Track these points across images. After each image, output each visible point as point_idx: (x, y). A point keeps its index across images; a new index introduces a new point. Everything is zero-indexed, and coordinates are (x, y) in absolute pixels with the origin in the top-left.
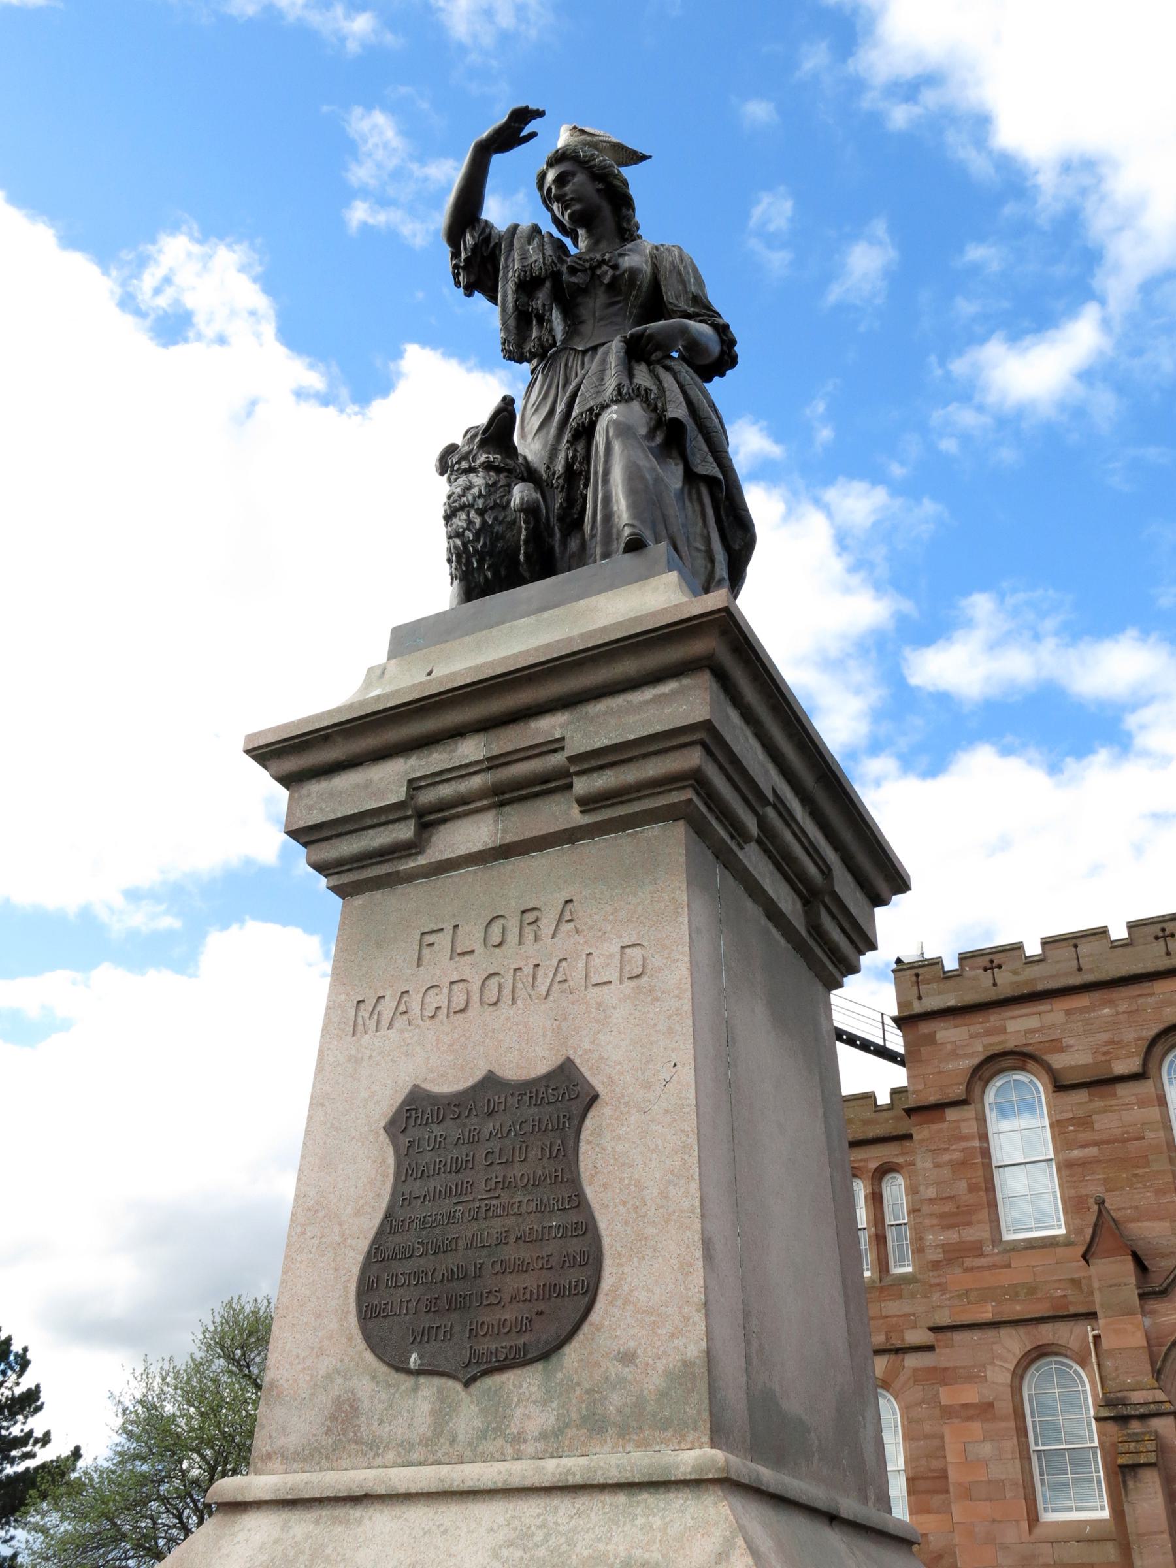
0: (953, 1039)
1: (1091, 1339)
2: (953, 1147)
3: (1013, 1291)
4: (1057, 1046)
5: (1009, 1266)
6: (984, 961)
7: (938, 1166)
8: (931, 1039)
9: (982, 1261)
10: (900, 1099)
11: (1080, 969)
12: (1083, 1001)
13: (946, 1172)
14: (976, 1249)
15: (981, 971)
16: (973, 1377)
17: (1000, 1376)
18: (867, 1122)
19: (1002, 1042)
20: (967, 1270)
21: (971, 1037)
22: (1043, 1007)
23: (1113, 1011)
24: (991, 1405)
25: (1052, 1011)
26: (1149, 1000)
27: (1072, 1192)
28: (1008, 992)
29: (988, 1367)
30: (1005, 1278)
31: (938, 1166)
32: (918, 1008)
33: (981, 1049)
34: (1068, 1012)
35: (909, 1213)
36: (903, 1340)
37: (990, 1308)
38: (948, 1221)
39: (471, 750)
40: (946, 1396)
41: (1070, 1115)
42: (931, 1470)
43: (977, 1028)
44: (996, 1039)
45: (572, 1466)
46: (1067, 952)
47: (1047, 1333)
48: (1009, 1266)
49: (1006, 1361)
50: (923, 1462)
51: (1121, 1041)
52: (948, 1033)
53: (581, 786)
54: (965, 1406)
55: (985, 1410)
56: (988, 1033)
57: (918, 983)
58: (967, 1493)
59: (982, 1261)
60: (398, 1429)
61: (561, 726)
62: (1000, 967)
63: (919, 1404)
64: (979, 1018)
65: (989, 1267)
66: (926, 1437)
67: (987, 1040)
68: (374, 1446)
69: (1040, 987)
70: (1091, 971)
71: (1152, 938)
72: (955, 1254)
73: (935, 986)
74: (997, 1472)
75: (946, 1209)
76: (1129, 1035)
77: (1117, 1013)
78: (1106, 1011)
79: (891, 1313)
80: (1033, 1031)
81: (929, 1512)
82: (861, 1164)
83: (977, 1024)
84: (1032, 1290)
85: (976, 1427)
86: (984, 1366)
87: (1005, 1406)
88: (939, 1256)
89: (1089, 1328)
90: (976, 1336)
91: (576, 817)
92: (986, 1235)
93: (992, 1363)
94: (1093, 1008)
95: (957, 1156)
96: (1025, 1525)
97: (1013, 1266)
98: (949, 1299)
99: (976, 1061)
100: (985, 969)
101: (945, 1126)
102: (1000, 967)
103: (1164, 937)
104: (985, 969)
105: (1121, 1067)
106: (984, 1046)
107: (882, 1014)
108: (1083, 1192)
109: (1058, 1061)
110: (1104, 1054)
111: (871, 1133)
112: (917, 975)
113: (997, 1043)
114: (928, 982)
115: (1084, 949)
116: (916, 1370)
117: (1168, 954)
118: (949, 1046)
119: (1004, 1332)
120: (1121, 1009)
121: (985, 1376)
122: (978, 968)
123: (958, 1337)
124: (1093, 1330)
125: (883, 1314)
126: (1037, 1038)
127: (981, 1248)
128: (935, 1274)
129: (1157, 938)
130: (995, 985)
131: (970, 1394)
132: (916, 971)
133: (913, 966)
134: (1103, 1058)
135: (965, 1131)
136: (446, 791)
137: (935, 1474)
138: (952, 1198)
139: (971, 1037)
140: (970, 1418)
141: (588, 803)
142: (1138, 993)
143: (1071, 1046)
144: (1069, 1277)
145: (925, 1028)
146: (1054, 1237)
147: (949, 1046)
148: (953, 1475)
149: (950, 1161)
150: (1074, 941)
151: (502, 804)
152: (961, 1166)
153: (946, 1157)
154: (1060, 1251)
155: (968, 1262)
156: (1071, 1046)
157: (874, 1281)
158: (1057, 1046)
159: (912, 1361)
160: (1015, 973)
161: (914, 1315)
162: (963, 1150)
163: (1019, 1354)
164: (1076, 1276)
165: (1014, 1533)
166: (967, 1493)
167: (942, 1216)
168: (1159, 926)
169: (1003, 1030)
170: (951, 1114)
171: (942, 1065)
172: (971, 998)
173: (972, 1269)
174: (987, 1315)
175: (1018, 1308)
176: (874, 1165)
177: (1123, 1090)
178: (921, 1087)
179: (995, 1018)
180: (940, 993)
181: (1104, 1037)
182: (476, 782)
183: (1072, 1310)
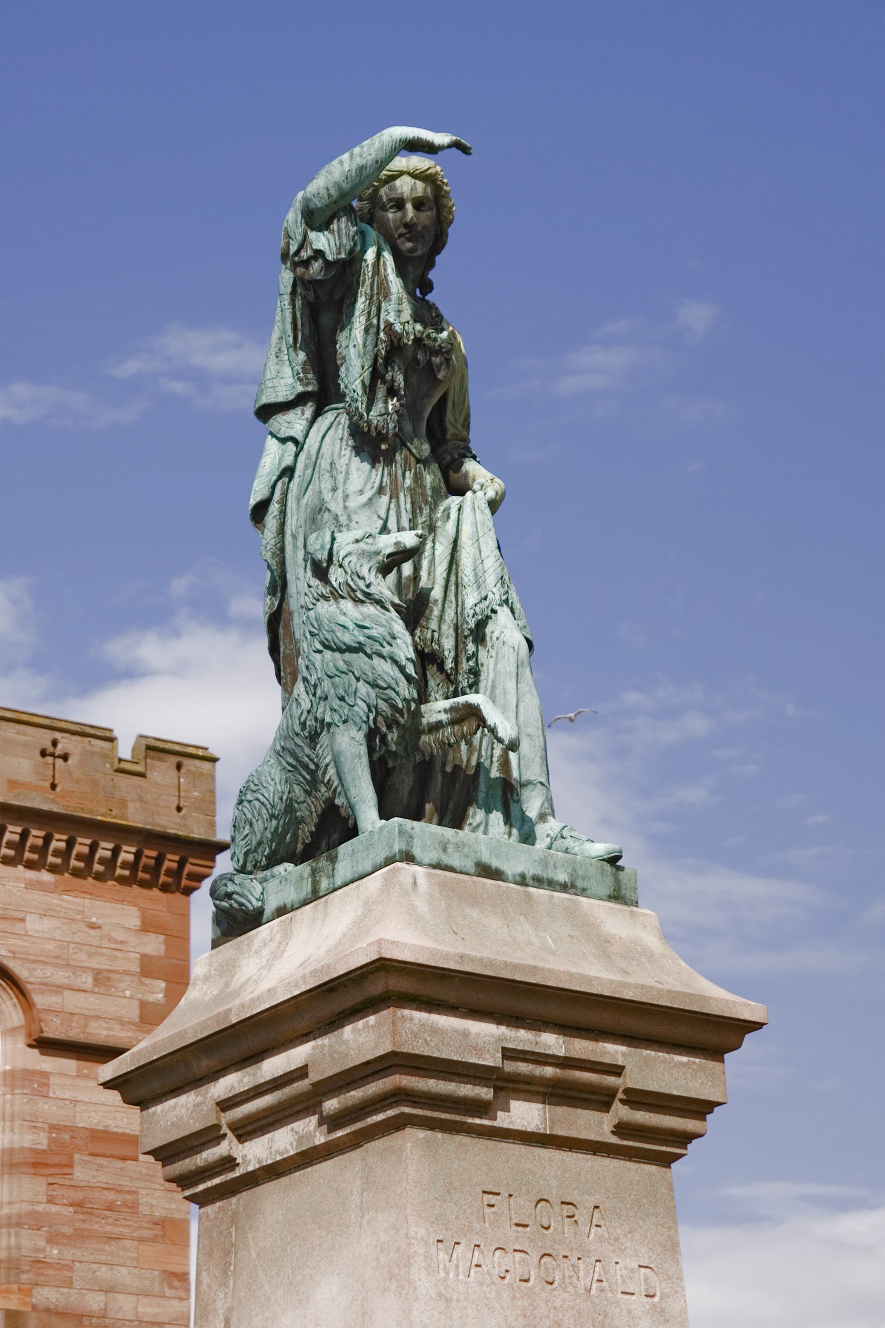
61: (624, 1055)
141: (622, 1129)
151: (551, 1095)
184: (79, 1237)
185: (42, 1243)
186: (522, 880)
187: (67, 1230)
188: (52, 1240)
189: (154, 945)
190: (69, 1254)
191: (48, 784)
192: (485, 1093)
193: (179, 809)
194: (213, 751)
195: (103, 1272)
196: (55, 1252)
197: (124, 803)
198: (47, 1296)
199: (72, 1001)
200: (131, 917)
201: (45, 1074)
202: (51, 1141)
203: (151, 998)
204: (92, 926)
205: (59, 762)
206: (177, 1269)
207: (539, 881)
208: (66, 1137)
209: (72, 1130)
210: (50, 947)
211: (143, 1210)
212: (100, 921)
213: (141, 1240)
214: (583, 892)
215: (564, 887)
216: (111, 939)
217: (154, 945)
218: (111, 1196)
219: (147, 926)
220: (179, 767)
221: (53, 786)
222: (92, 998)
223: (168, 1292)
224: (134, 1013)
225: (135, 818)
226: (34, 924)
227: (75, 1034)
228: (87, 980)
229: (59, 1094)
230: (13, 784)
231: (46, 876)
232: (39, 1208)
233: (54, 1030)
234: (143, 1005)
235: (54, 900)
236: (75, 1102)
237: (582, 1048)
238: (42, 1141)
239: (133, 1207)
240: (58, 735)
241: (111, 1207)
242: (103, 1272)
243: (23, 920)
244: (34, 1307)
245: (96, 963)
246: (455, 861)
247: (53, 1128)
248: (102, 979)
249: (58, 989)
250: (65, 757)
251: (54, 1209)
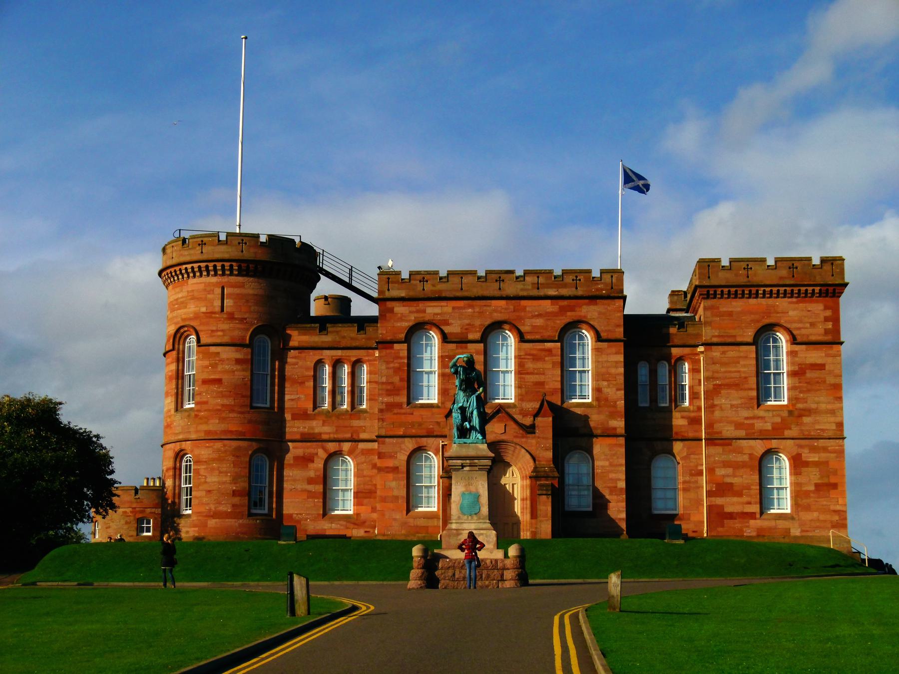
0: (402, 312)
1: (441, 446)
2: (395, 361)
3: (412, 425)
4: (447, 323)
5: (412, 414)
6: (419, 277)
7: (388, 368)
8: (391, 310)
9: (403, 411)
10: (369, 330)
11: (462, 289)
12: (461, 303)
13: (391, 371)
14: (399, 405)
15: (418, 282)
16: (392, 456)
17: (403, 457)
18: (352, 339)
19: (422, 317)
20: (395, 414)
21: (411, 312)
22: (443, 303)
23: (473, 311)
24: (397, 468)
25: (447, 306)
26: (488, 308)
27: (443, 386)
28: (430, 295)
29: (398, 454)
30: (410, 419)
31: (388, 368)
32: (388, 295)
33: (413, 318)
34: (454, 308)
35: (367, 382)
36: (359, 437)
37: (402, 430)
38: (389, 393)
39: (468, 461)
40: (379, 463)
41: (447, 354)
42: (365, 489)
43: (413, 309)
44: (421, 315)
45: (477, 522)
46: (456, 280)
47: (424, 441)
48: (412, 414)
49: (405, 451)
50: (362, 486)
51: (473, 325)
52: (400, 309)
53: (478, 467)
54: (387, 468)
55: (395, 469)
56: (418, 312)
57: (389, 282)
58: (384, 500)
59: (403, 411)
60: (464, 518)
62: (427, 281)
63: (363, 463)
64: (415, 303)
65: (404, 414)
66: (364, 476)
67: (416, 315)
68: (462, 519)
69: (443, 295)
70: (467, 291)
71: (495, 281)
72: (390, 407)
73: (396, 285)
74: (396, 493)
75: (389, 387)
76: (478, 322)
77: (474, 312)
78: (470, 310)
79: (355, 425)
80: (437, 314)
81: (362, 505)
82: (347, 358)
83: (414, 306)
84: (420, 424)
85: (391, 476)
86: (397, 453)
87: (403, 468)
88: (384, 407)
89: (441, 441)
90: (395, 440)
91: (477, 470)
92: (405, 400)
93: (400, 452)
94: (464, 308)
95: (397, 365)
96: (405, 512)
97: (414, 414)
98: (386, 425)
99: (411, 324)
100: (420, 281)
101: (393, 351)
102: (427, 281)
103: (500, 281)
104: (420, 281)
105: (471, 337)
106: (415, 317)
107: (352, 267)
108: (447, 387)
109: (447, 329)
110: (466, 329)
111: (354, 344)
112: (389, 278)
113: (421, 317)
114: (393, 282)
115: (464, 280)
116: (363, 450)
117: (500, 289)
118: (399, 315)
119: (406, 440)
120: (477, 310)
121: (396, 457)
122: (417, 280)
123: (387, 440)
124: (442, 442)
125: (351, 425)
126: (439, 317)
127: (402, 405)
128: (381, 414)
129: (497, 281)
130: (424, 289)
131: (391, 463)
132: (388, 276)
133: (387, 273)
134: (465, 331)
135: (401, 355)
136: (465, 464)
137: (367, 491)
138: (392, 383)
139: (411, 312)
140: (388, 472)
141: (479, 469)
142: (484, 304)
143: (453, 324)
144: (436, 420)
145: (389, 304)
146: (432, 404)
147: (399, 315)
148: (379, 493)
149: (393, 367)
150: (461, 275)
152: (397, 370)
153: (392, 365)
154: (434, 410)
155: (396, 411)
156: (453, 324)
157: (348, 411)
158: (447, 323)
159: (361, 446)
160: (434, 285)
161: (365, 427)
162: (399, 363)
163: (411, 449)
164: (439, 421)
165: (400, 515)
166: (384, 500)
167: (387, 390)
168: (499, 275)
169: (424, 311)
170: (396, 346)
171: (395, 323)
172: (412, 294)
173: (397, 414)
174: (401, 433)
175: (414, 431)
176: (354, 359)
177: (469, 345)
178: (384, 332)
179: (421, 305)
180: (399, 289)
181: (467, 321)
182: (468, 464)
183: (435, 434)
184: (809, 391)
185: (798, 393)
186: (470, 443)
187: (805, 389)
188: (800, 392)
189: (829, 313)
190: (806, 396)
191: (791, 276)
192: (461, 467)
193: (833, 275)
194: (844, 257)
195: (816, 399)
196: (802, 395)
197: (815, 277)
198: (800, 406)
199: (803, 331)
200: (820, 306)
201: (797, 351)
202: (799, 368)
203: (828, 327)
204: (809, 311)
205: (795, 270)
206: (839, 396)
207: (472, 443)
208: (803, 366)
209: (806, 364)
210: (796, 318)
211: (828, 382)
212: (811, 309)
213: (827, 390)
214: (478, 443)
215: (475, 443)
216: (814, 313)
217: (829, 313)
218: (817, 380)
219: (826, 308)
220: (832, 264)
221: (793, 276)
222: (810, 330)
223: (836, 402)
224: (822, 331)
225: (819, 280)
226: (791, 313)
227: (805, 339)
228: (808, 325)
229: (801, 356)
230: (781, 278)
231: (794, 300)
232: (797, 385)
233: (799, 339)
234: (825, 329)
235: (797, 305)
236: (806, 357)
237: (472, 461)
238: (796, 368)
239: (825, 382)
240: (794, 262)
241: (818, 382)
242: (816, 399)
243: (788, 312)
244: (796, 409)
245: (814, 320)
246: (461, 443)
247: (799, 364)
248: (813, 325)
249: (799, 329)
250: (797, 268)
251: (801, 384)
